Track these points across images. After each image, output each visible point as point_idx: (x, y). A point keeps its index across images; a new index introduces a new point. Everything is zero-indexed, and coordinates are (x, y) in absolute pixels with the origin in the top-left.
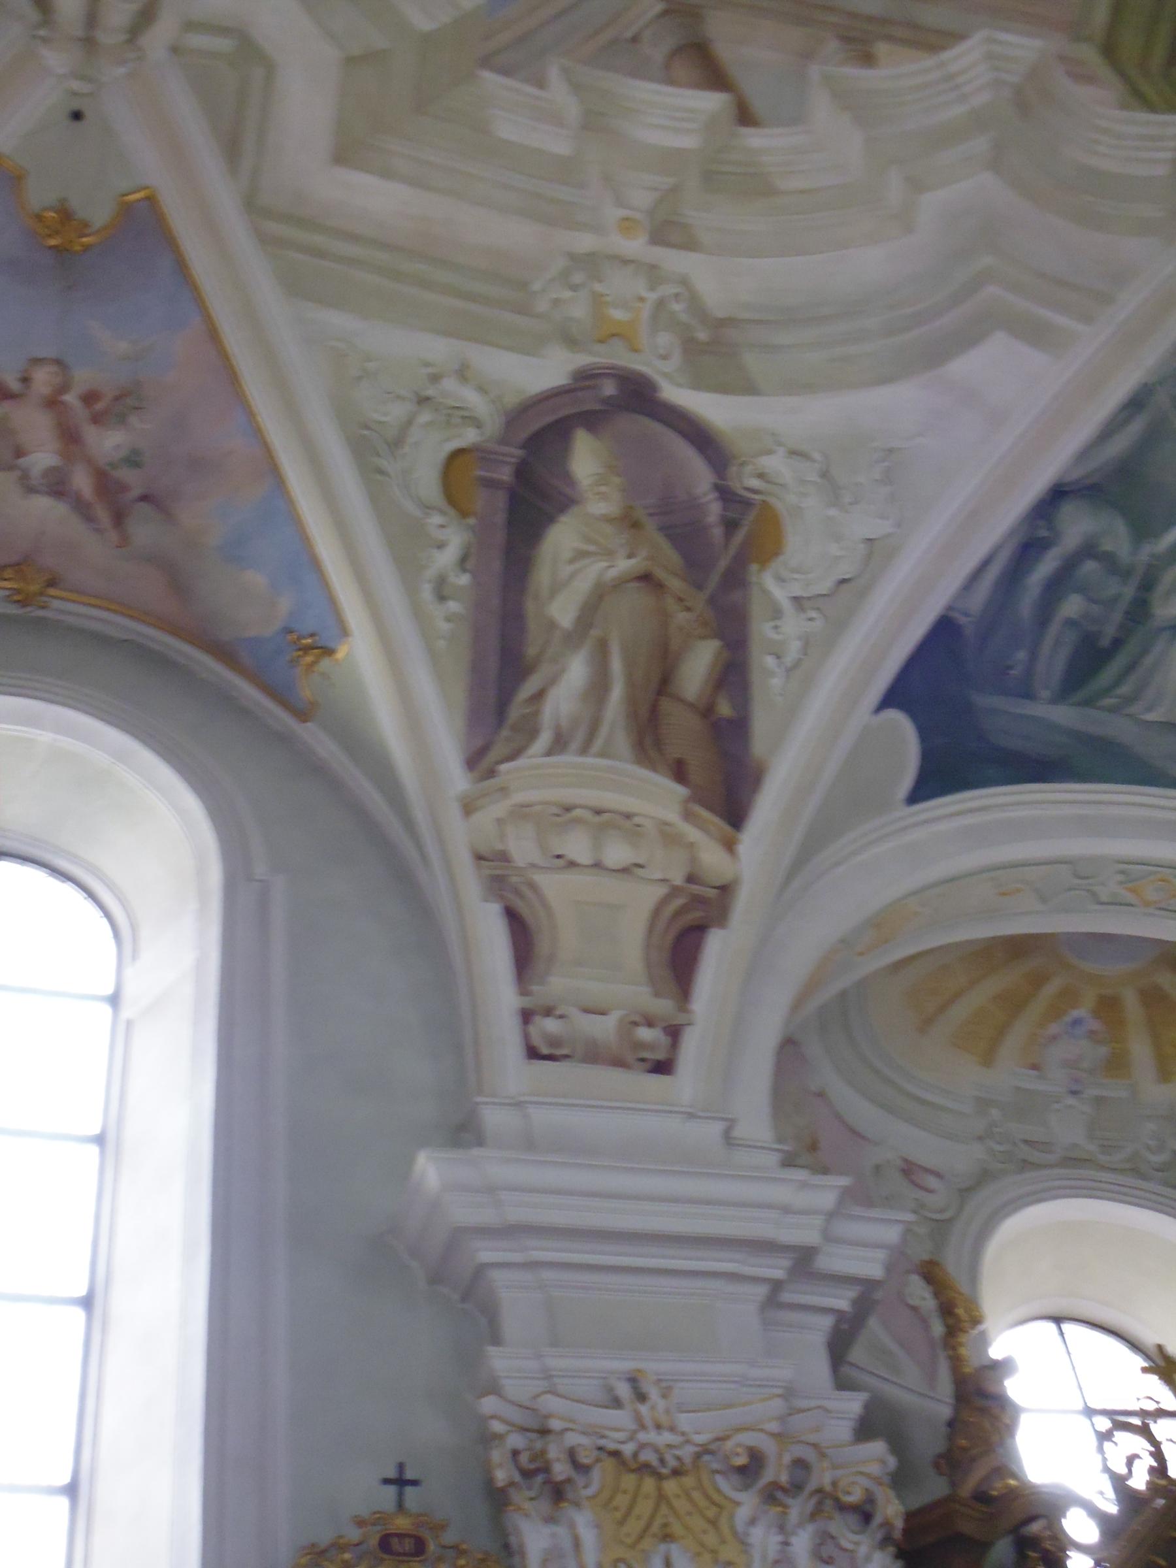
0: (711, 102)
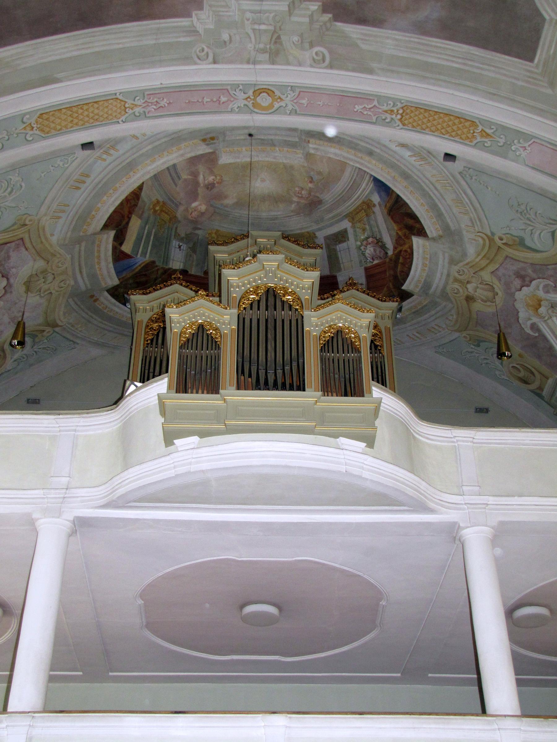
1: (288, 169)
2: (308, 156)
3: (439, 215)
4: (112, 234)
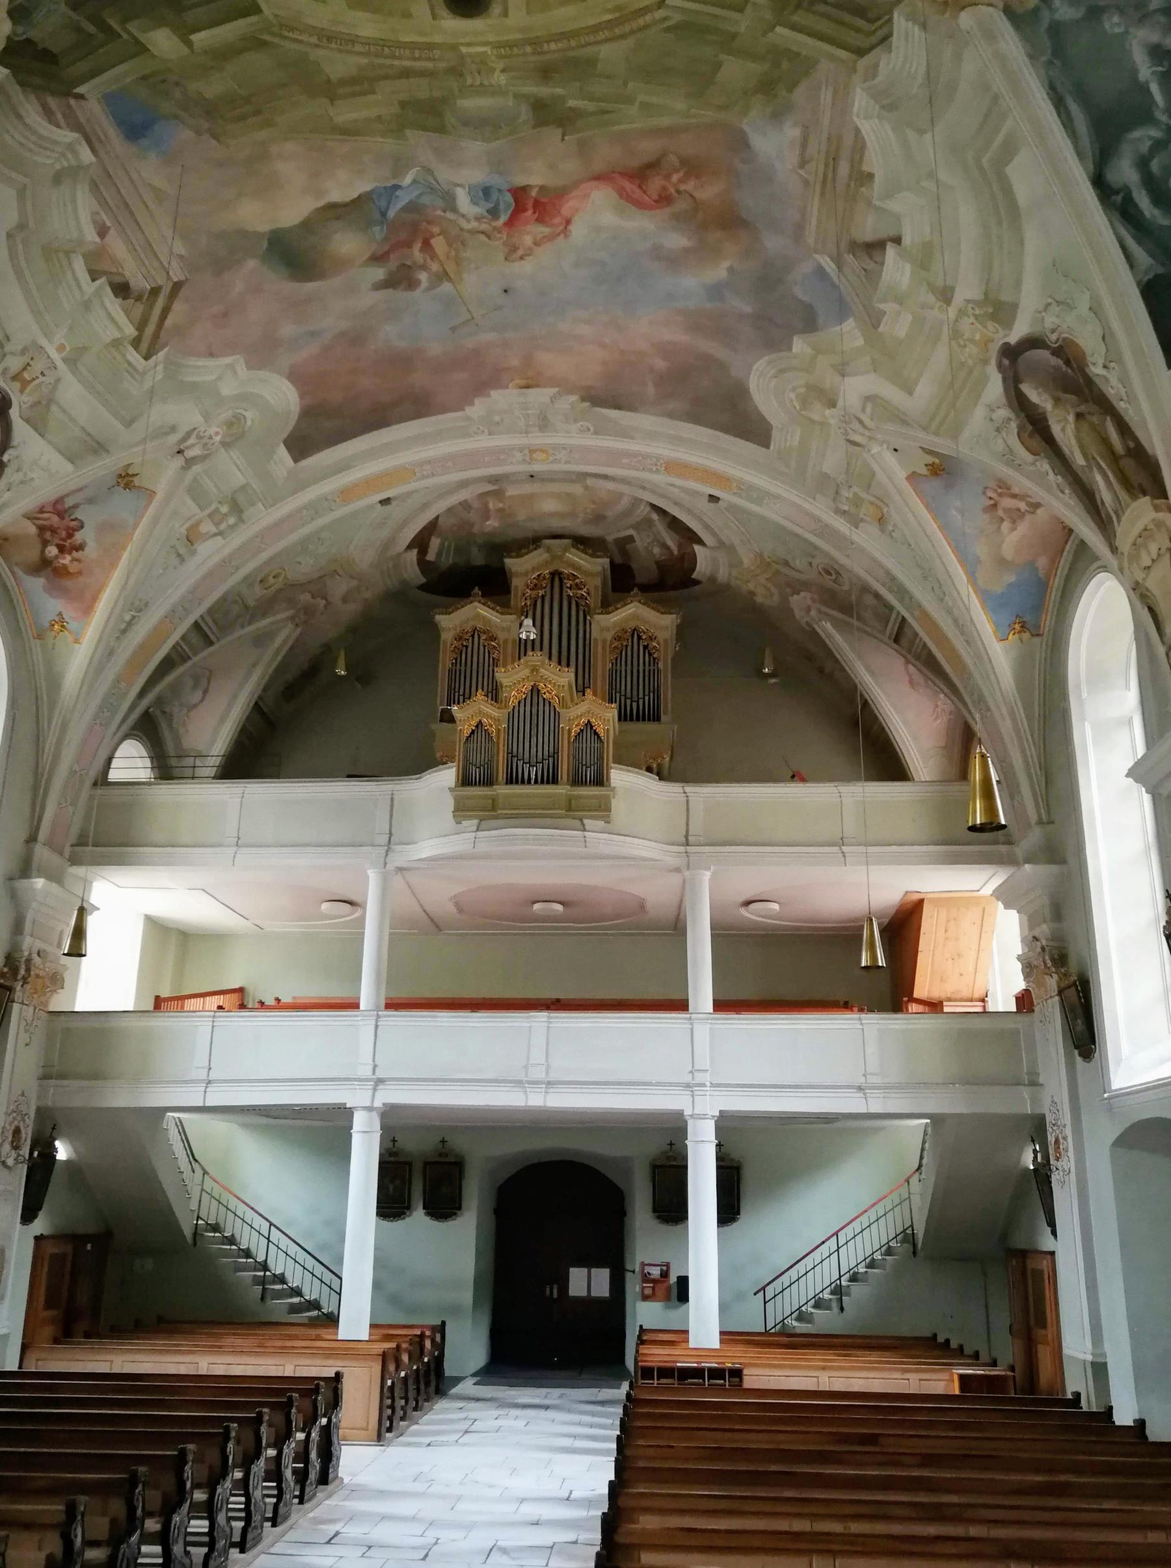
0: (891, 251)
2: (586, 488)
3: (714, 534)
4: (415, 551)
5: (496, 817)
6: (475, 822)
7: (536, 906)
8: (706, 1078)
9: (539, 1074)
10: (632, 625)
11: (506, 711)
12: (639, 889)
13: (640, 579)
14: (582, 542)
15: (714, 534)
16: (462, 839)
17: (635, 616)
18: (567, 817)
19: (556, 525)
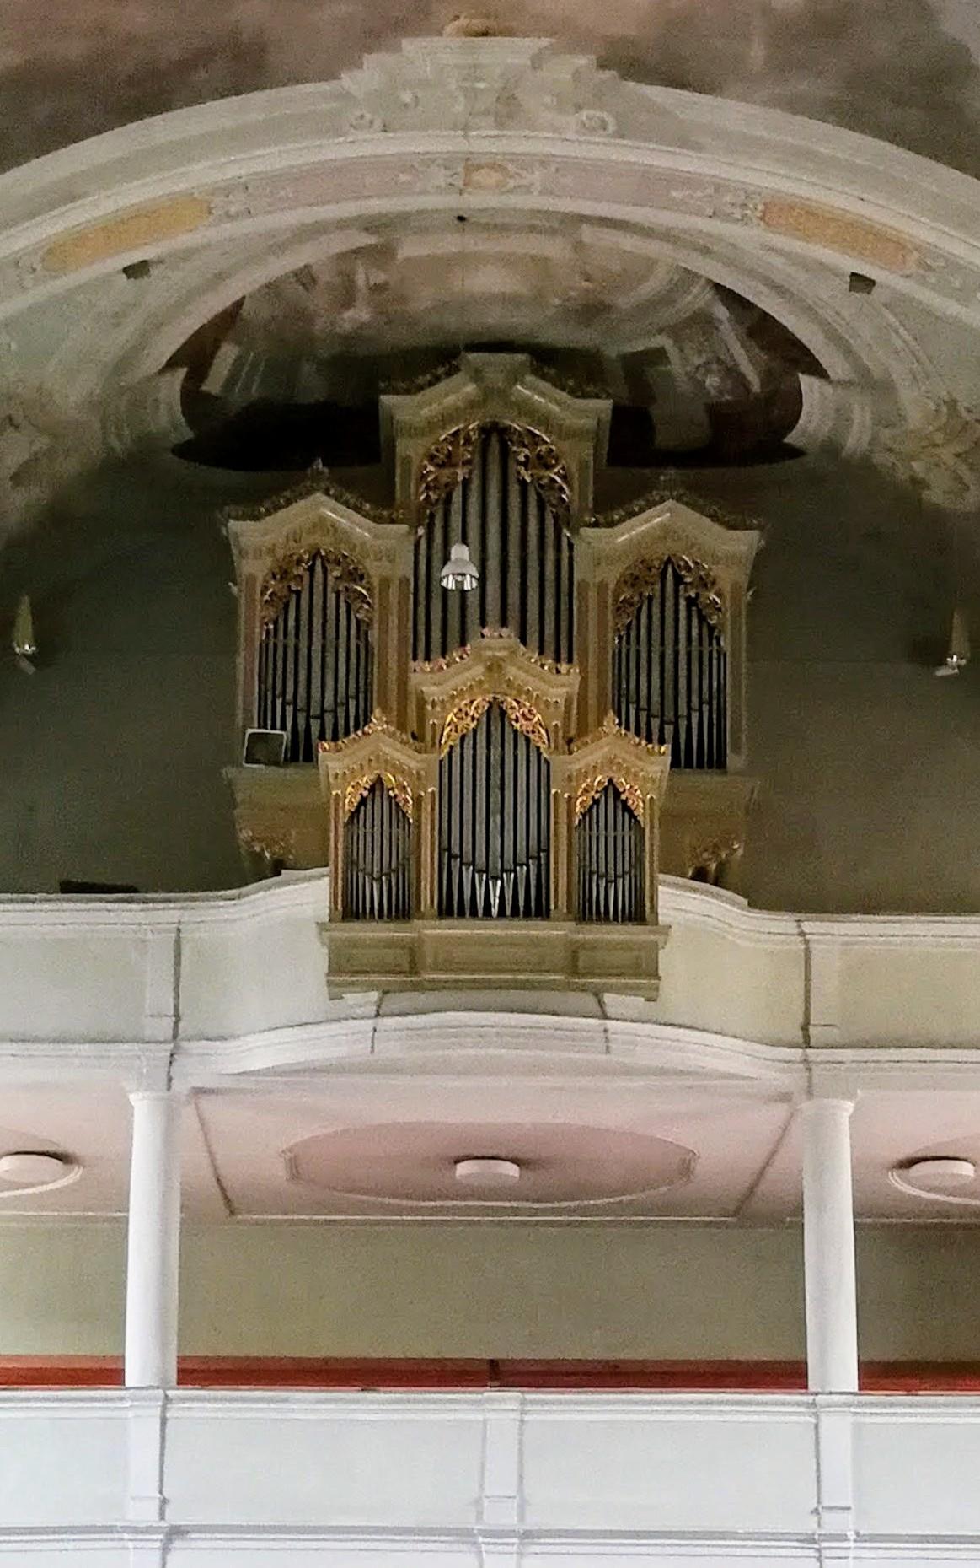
1: (542, 263)
3: (848, 352)
4: (182, 372)
5: (417, 987)
6: (374, 995)
7: (463, 1169)
8: (845, 1523)
9: (508, 1518)
10: (663, 551)
11: (434, 758)
12: (685, 1136)
13: (664, 438)
14: (549, 360)
15: (848, 352)
16: (350, 1033)
17: (666, 532)
18: (568, 987)
19: (495, 319)
